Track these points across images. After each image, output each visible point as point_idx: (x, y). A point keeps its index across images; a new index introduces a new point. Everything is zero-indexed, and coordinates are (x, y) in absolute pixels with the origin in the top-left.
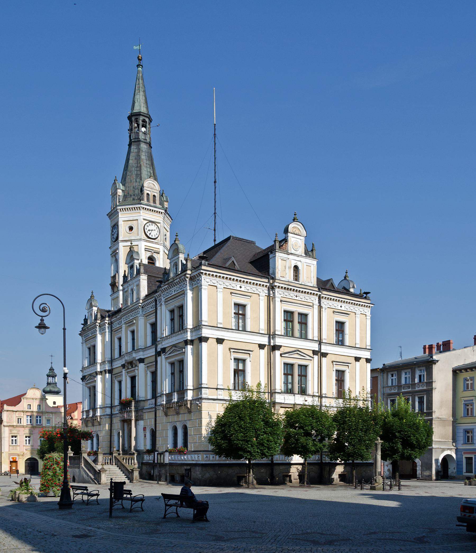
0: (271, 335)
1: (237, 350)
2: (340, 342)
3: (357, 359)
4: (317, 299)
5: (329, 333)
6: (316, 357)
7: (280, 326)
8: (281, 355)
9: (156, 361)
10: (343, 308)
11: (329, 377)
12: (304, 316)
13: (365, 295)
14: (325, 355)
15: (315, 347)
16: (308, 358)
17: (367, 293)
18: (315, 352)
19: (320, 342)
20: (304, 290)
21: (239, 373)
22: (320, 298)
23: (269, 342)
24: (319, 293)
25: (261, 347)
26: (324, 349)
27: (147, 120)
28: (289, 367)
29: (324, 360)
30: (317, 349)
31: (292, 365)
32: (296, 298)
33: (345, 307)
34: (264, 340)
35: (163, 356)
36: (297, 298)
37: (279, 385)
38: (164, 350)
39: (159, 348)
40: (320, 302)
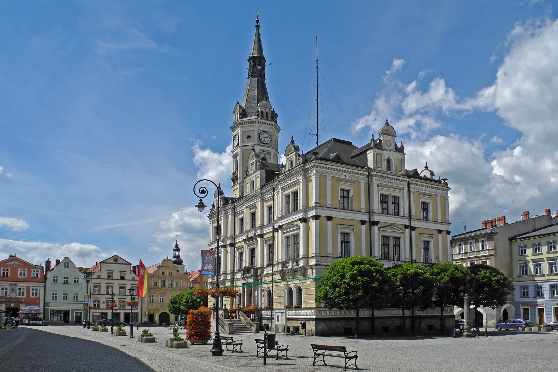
0: (370, 212)
2: (426, 218)
3: (440, 231)
5: (417, 212)
6: (407, 231)
7: (377, 205)
8: (379, 228)
9: (273, 237)
11: (417, 246)
14: (414, 228)
15: (407, 222)
16: (401, 231)
18: (406, 227)
23: (370, 219)
25: (363, 223)
26: (413, 224)
28: (385, 239)
29: (413, 232)
30: (408, 224)
34: (365, 218)
37: (377, 253)
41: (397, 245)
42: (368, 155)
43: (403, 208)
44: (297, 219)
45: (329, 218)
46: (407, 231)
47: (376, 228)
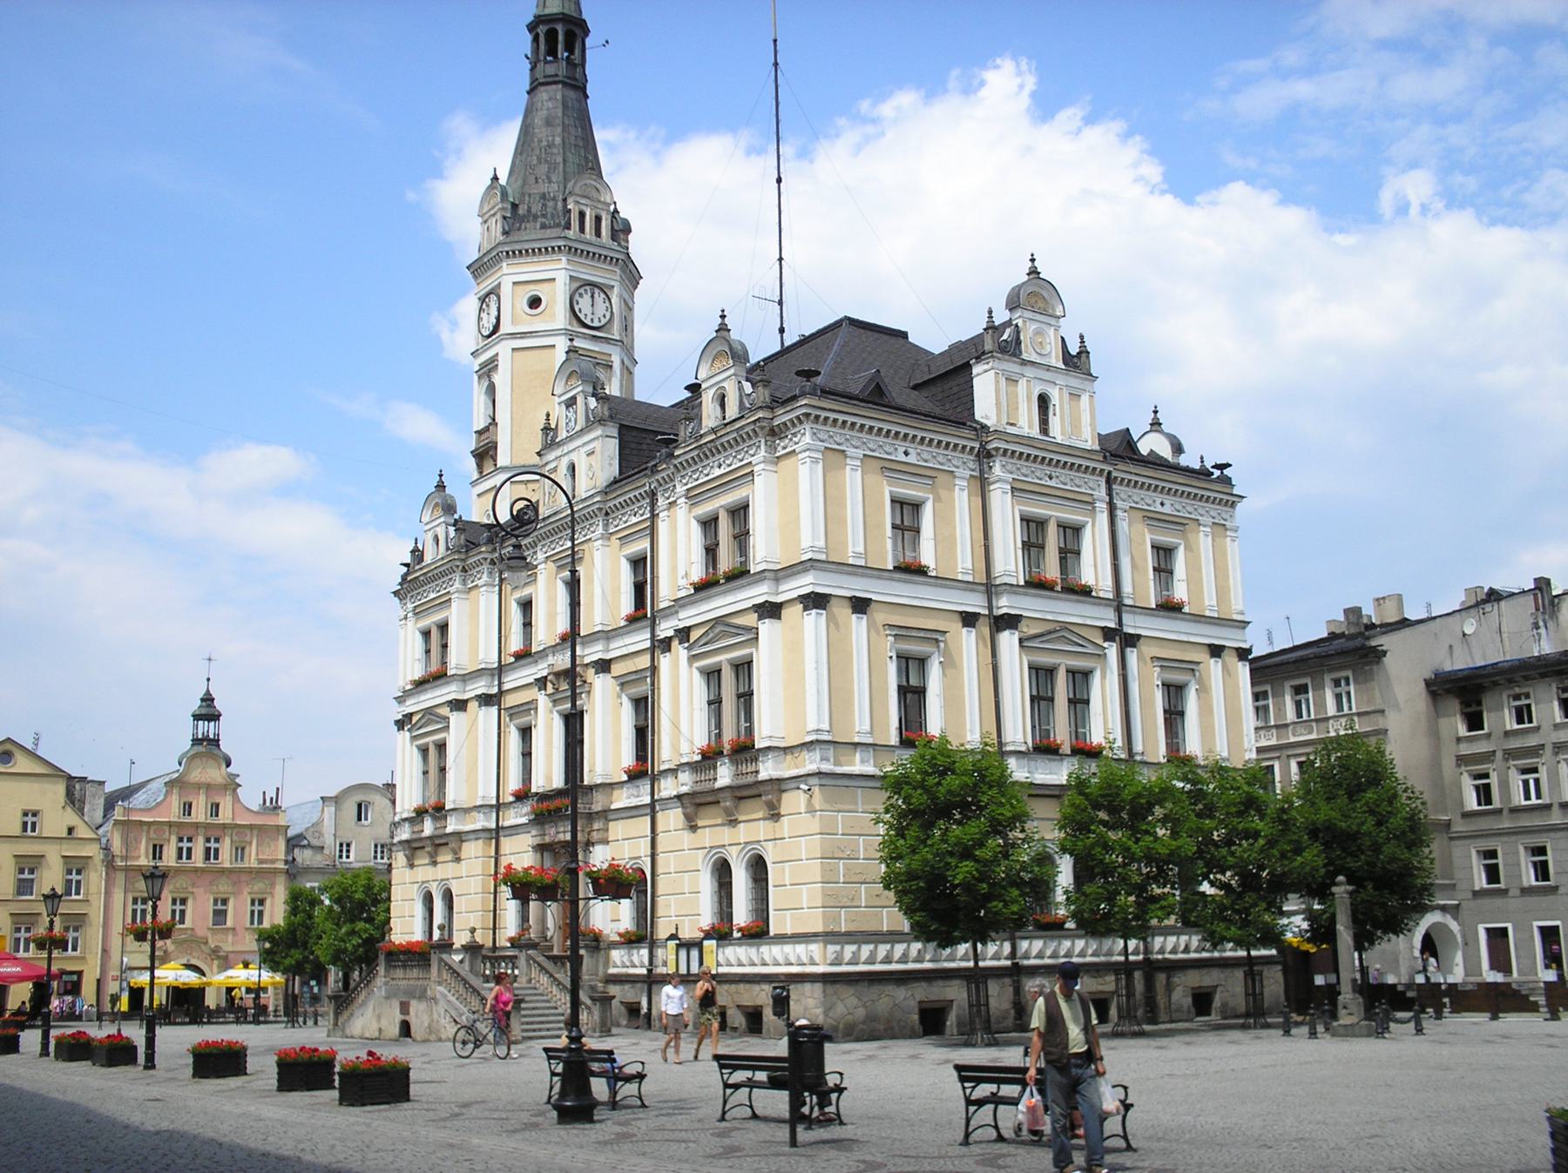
1: (901, 632)
2: (1170, 608)
4: (1103, 484)
8: (1021, 641)
10: (1167, 509)
12: (1072, 531)
13: (1217, 473)
14: (1130, 641)
17: (1221, 467)
18: (1108, 634)
19: (1119, 605)
20: (1070, 460)
21: (912, 696)
22: (1110, 481)
23: (990, 607)
24: (1107, 468)
25: (969, 619)
26: (1132, 624)
27: (578, 31)
28: (1042, 675)
29: (1132, 655)
30: (1112, 625)
31: (1051, 672)
32: (1049, 483)
33: (1170, 507)
34: (975, 603)
35: (680, 651)
36: (1052, 483)
37: (1018, 731)
38: (684, 634)
39: (666, 629)
40: (1110, 493)
41: (1079, 703)
42: (975, 381)
43: (1093, 569)
44: (749, 604)
45: (860, 605)
46: (1112, 650)
47: (1008, 641)
